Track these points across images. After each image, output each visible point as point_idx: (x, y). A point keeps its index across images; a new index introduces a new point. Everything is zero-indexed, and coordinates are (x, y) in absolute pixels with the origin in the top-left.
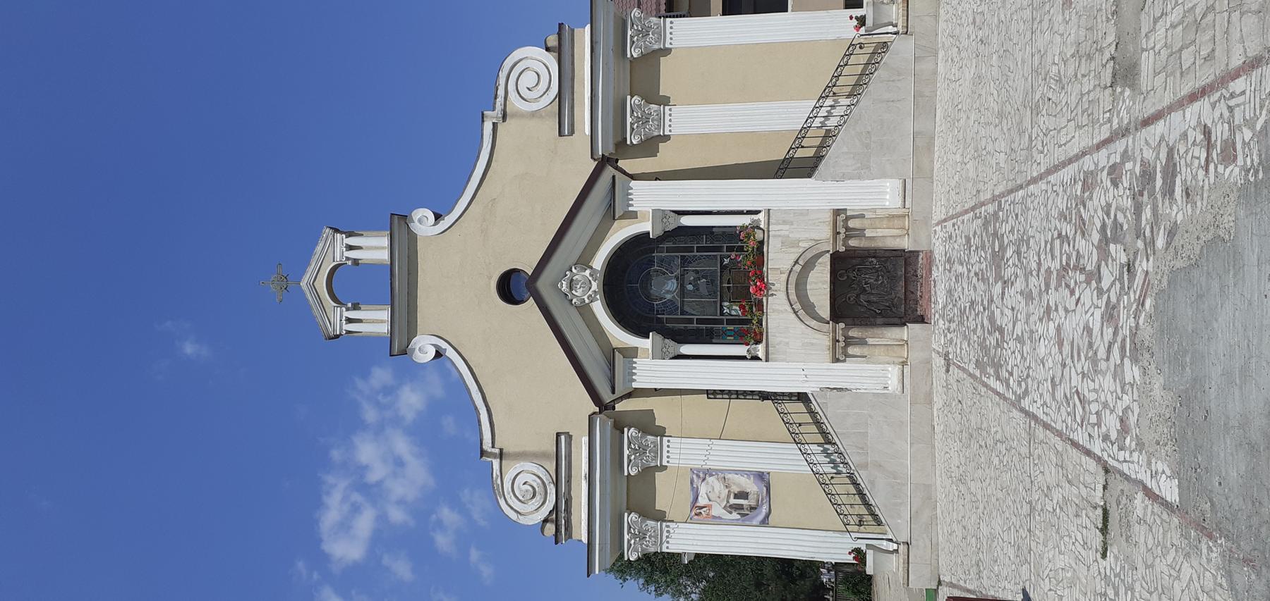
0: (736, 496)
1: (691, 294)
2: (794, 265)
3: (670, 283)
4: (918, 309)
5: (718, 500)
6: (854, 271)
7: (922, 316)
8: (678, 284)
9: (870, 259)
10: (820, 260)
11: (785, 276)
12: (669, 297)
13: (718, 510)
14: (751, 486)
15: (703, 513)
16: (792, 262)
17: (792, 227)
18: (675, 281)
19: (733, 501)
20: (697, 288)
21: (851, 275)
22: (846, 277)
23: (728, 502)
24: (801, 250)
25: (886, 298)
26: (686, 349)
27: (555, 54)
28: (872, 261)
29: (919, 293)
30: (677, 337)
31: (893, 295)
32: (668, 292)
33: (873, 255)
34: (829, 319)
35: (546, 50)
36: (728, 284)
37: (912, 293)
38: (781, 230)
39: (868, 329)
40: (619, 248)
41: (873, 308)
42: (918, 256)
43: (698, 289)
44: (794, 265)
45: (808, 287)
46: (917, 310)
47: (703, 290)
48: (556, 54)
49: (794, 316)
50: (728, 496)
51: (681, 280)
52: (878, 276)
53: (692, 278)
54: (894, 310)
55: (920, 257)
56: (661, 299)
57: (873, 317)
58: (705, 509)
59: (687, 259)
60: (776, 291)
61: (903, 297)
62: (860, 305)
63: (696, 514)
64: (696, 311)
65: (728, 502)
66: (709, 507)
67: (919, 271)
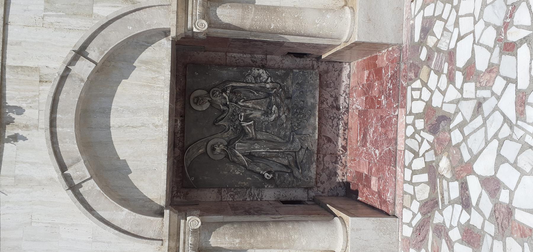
2: (74, 60)
4: (339, 172)
6: (224, 91)
7: (347, 185)
9: (256, 72)
10: (147, 54)
11: (49, 90)
16: (67, 54)
21: (218, 100)
22: (207, 105)
24: (94, 25)
25: (284, 149)
28: (260, 76)
29: (341, 142)
31: (297, 144)
33: (259, 63)
34: (162, 202)
37: (329, 140)
39: (255, 230)
41: (258, 169)
42: (341, 71)
44: (74, 60)
45: (114, 121)
46: (336, 174)
49: (68, 197)
52: (270, 105)
54: (297, 173)
55: (345, 73)
57: (258, 188)
60: (26, 127)
61: (315, 148)
62: (234, 162)
67: (341, 100)
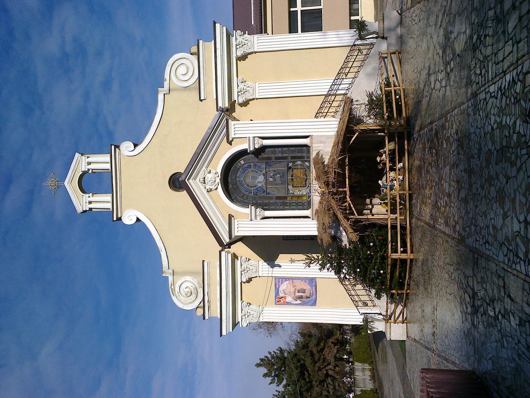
1: (271, 183)
3: (260, 177)
5: (289, 294)
8: (264, 177)
12: (260, 185)
13: (289, 299)
14: (307, 287)
15: (282, 301)
17: (325, 144)
18: (262, 176)
20: (275, 179)
23: (295, 294)
26: (268, 213)
27: (196, 56)
30: (265, 207)
32: (259, 182)
35: (191, 54)
36: (292, 177)
38: (319, 146)
40: (231, 159)
43: (275, 180)
47: (279, 181)
48: (197, 56)
50: (295, 292)
51: (265, 175)
53: (272, 174)
56: (256, 186)
58: (282, 299)
59: (269, 164)
63: (278, 302)
64: (276, 192)
65: (295, 294)
66: (285, 298)
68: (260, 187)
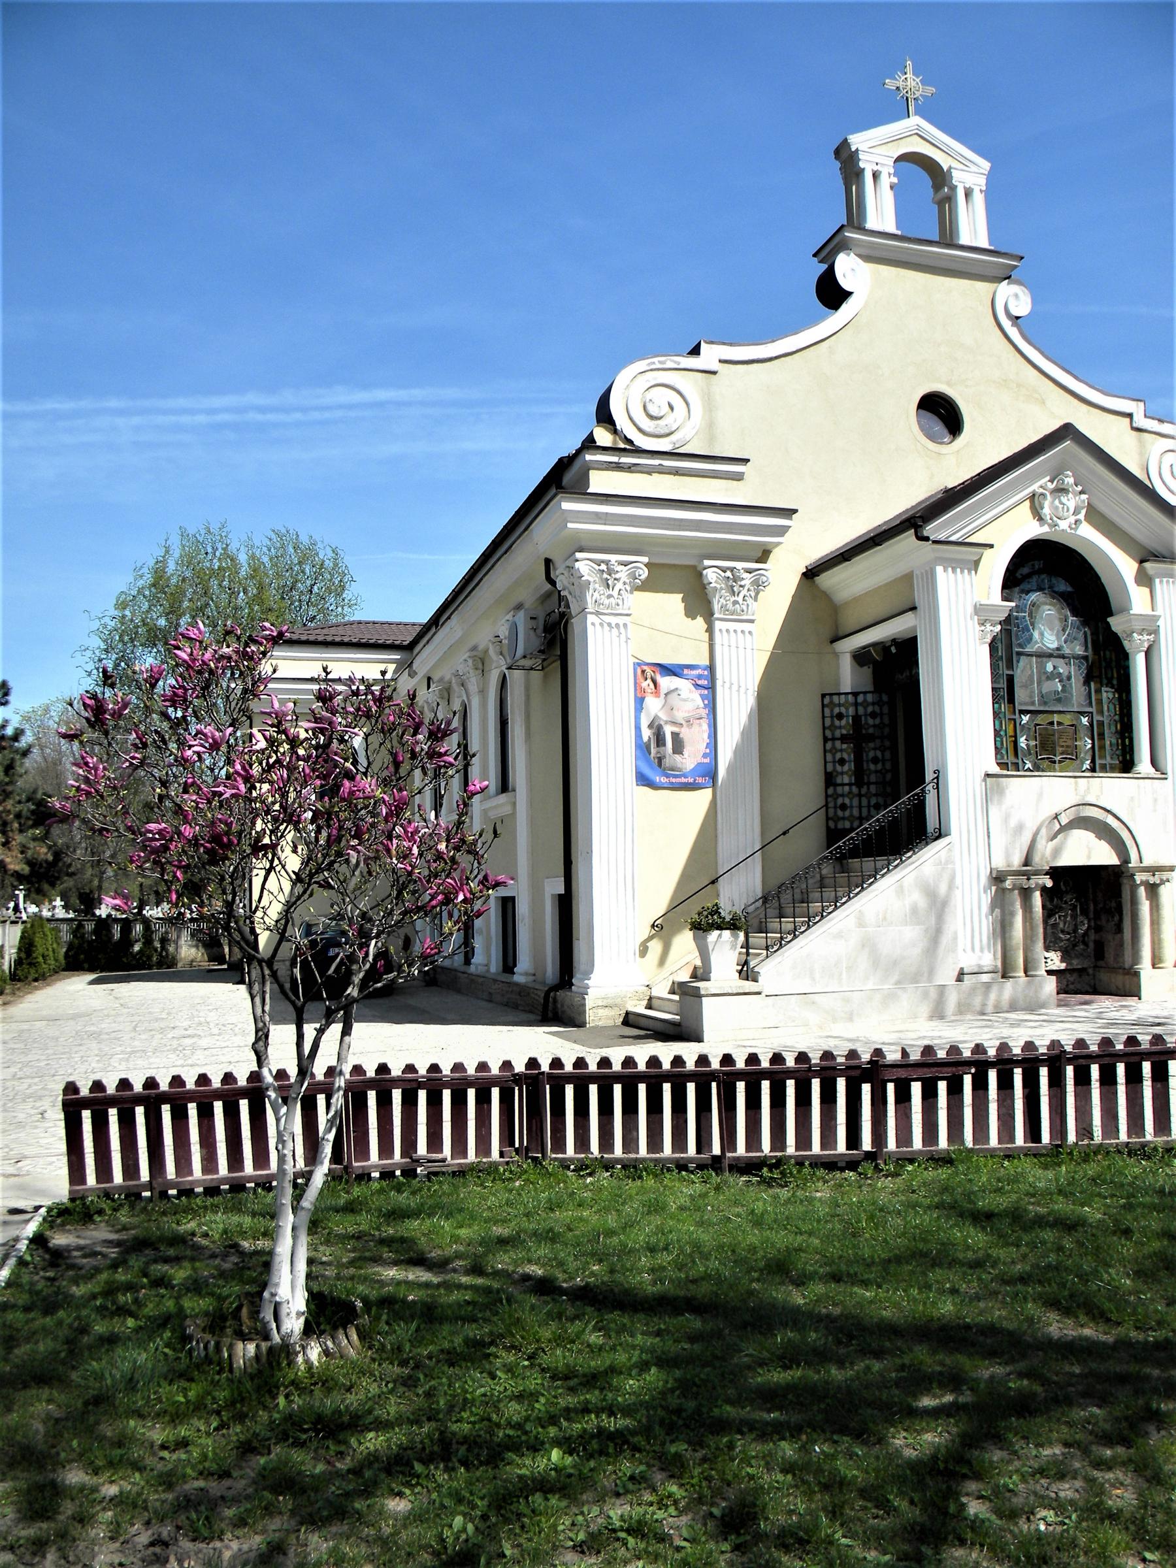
0: (675, 736)
1: (1041, 667)
12: (1036, 635)
13: (653, 705)
19: (668, 730)
20: (1050, 677)
32: (1042, 634)
43: (1048, 678)
47: (1048, 687)
56: (1033, 624)
58: (652, 685)
63: (643, 672)
65: (666, 722)
68: (1031, 636)
